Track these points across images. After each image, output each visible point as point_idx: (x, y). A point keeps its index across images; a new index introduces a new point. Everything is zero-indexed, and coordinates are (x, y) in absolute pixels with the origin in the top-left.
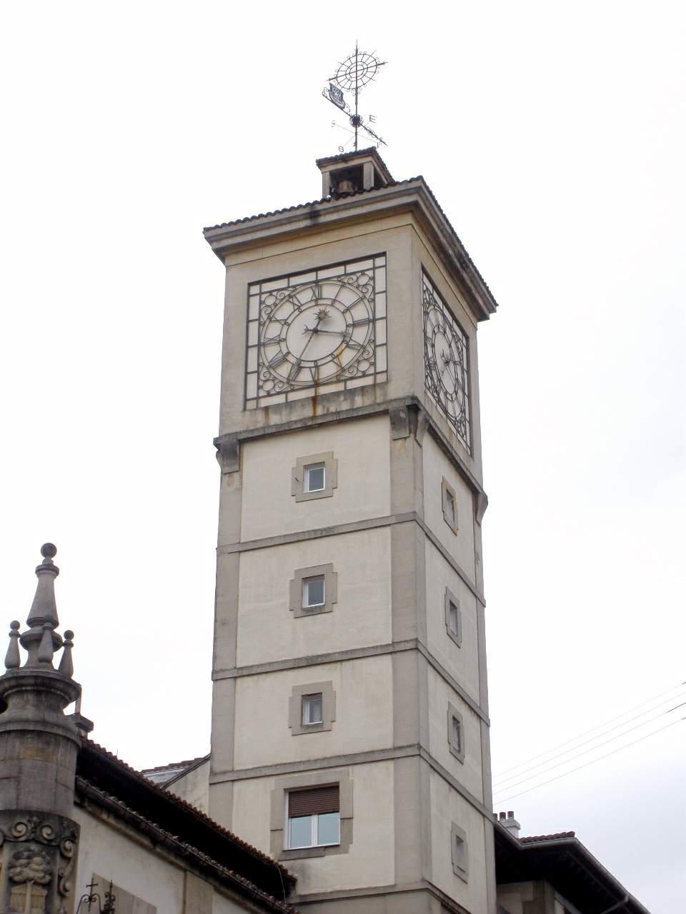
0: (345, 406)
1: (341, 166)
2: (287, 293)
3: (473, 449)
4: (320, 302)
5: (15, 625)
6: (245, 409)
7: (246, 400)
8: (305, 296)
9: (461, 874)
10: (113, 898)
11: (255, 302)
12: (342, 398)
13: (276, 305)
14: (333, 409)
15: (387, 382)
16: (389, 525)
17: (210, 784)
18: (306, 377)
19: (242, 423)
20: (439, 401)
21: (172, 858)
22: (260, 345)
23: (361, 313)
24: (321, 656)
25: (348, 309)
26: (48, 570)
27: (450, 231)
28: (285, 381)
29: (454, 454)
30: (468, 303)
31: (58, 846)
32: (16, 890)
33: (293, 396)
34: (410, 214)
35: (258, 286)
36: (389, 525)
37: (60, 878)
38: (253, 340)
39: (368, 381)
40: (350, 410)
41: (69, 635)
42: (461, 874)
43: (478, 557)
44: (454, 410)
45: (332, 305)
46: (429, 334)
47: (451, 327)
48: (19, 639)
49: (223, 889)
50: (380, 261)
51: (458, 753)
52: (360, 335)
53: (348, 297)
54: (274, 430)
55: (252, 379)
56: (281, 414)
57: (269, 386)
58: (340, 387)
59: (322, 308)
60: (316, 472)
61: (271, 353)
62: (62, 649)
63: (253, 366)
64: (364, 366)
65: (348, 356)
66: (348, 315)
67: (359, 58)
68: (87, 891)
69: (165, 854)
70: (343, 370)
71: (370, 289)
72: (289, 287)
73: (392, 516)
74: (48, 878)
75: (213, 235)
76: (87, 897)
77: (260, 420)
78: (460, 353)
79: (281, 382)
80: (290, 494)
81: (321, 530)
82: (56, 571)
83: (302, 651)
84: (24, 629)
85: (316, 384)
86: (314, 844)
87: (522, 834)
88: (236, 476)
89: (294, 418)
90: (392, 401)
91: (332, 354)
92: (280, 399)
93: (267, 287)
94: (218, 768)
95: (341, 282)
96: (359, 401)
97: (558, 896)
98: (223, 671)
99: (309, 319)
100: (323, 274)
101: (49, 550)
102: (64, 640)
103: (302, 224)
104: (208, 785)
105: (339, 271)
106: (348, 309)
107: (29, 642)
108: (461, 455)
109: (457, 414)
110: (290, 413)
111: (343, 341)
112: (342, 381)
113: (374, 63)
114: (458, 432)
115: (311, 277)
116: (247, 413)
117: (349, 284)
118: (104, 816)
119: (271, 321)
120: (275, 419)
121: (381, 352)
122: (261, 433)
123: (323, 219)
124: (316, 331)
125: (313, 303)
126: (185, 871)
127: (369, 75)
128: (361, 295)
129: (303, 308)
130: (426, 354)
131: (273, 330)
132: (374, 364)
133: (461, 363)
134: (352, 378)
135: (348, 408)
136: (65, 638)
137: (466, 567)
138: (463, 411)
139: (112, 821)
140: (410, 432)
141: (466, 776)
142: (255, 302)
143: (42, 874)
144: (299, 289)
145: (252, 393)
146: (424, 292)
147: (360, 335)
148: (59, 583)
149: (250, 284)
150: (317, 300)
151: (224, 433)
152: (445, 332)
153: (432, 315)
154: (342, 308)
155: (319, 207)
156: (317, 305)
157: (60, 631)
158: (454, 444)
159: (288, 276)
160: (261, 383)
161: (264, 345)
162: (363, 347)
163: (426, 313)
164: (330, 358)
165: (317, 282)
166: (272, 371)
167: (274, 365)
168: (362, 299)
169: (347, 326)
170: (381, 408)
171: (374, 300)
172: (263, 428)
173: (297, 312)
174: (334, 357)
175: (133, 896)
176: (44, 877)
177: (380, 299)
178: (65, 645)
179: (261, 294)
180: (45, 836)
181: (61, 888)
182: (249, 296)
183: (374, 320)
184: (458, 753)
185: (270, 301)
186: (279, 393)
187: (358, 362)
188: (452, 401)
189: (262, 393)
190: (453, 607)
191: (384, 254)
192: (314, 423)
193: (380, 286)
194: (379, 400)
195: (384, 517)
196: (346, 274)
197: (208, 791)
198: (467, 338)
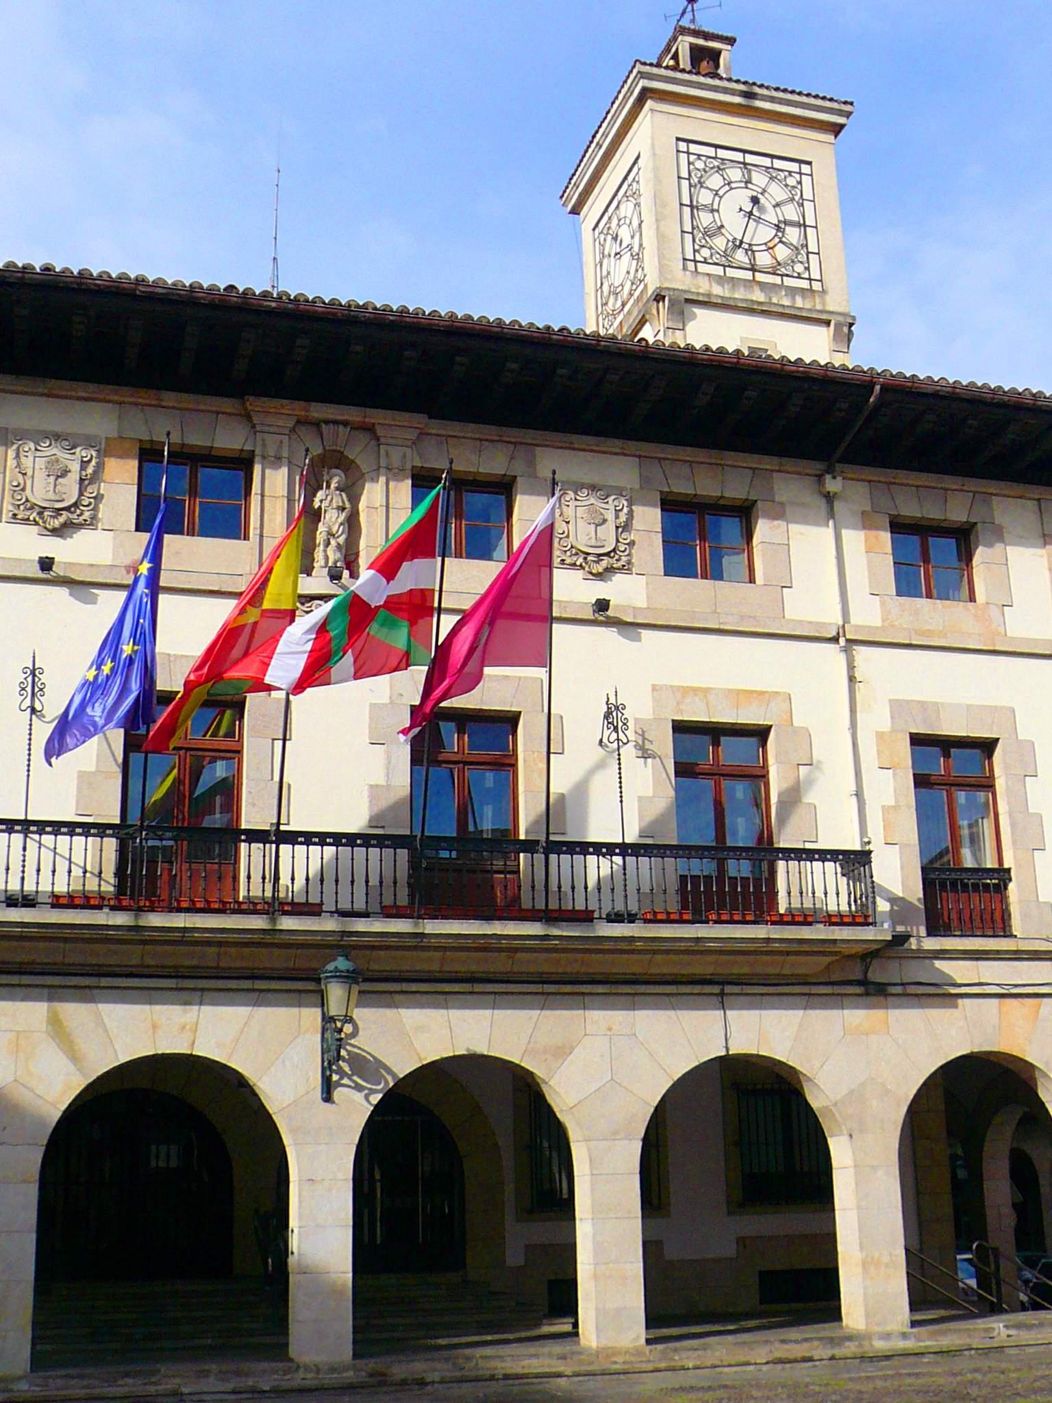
0: (786, 302)
1: (701, 42)
8: (735, 174)
14: (775, 300)
23: (791, 212)
25: (777, 205)
33: (731, 272)
38: (686, 201)
39: (804, 284)
50: (806, 169)
53: (777, 192)
54: (720, 301)
57: (705, 253)
63: (688, 228)
65: (782, 253)
66: (778, 209)
77: (703, 287)
90: (832, 313)
91: (765, 244)
92: (719, 271)
93: (694, 148)
96: (799, 302)
99: (742, 198)
100: (750, 159)
103: (738, 100)
111: (776, 235)
112: (778, 275)
119: (702, 186)
120: (717, 290)
125: (743, 185)
144: (729, 164)
147: (793, 234)
149: (678, 139)
150: (746, 183)
154: (774, 203)
155: (757, 90)
159: (717, 147)
160: (697, 247)
162: (797, 249)
164: (764, 247)
167: (708, 233)
168: (792, 200)
172: (709, 295)
182: (678, 151)
191: (810, 163)
193: (808, 194)
194: (819, 307)
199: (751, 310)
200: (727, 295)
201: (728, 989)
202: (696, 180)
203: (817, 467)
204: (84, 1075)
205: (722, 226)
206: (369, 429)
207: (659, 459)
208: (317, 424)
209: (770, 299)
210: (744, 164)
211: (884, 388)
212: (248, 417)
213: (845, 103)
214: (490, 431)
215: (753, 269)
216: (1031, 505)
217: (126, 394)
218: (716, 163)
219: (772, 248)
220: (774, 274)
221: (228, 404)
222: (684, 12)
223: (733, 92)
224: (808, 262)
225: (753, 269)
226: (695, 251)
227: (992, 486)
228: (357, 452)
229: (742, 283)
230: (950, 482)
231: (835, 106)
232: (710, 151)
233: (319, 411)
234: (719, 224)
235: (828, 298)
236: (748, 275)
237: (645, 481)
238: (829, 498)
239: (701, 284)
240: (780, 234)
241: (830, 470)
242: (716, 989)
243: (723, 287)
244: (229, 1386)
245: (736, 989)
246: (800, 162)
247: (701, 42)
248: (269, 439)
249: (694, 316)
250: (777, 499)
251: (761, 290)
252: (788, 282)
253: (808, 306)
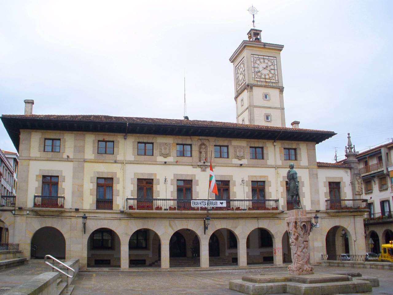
0: (272, 85)
1: (255, 32)
8: (262, 60)
14: (269, 85)
23: (272, 67)
26: (349, 138)
50: (275, 58)
57: (256, 76)
58: (270, 81)
64: (274, 78)
65: (271, 75)
77: (256, 83)
88: (252, 92)
93: (254, 56)
96: (274, 85)
100: (265, 57)
101: (349, 134)
103: (262, 46)
107: (348, 148)
120: (259, 83)
123: (266, 47)
124: (265, 68)
147: (272, 72)
168: (272, 65)
194: (277, 86)
199: (265, 87)
200: (261, 84)
201: (259, 219)
203: (273, 141)
204: (174, 231)
206: (208, 139)
207: (250, 141)
208: (201, 139)
210: (264, 58)
211: (283, 132)
212: (191, 139)
214: (225, 139)
215: (265, 79)
216: (306, 144)
217: (174, 137)
220: (269, 79)
221: (188, 137)
225: (265, 79)
227: (299, 142)
228: (206, 143)
230: (293, 142)
232: (257, 56)
233: (200, 137)
235: (279, 84)
236: (264, 80)
237: (247, 145)
238: (275, 146)
241: (275, 142)
242: (257, 219)
244: (194, 270)
245: (260, 219)
246: (274, 57)
248: (194, 142)
250: (267, 146)
253: (276, 85)
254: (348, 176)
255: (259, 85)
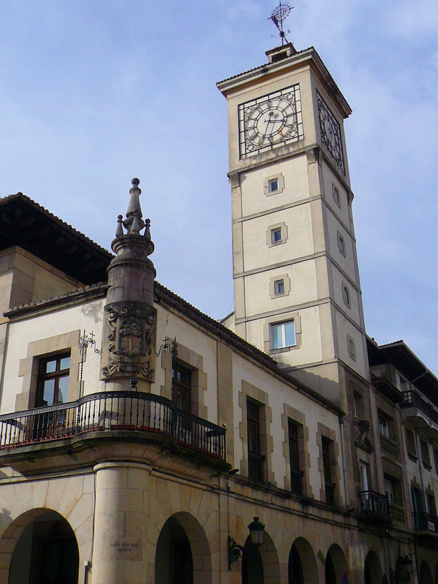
0: (285, 152)
1: (277, 53)
2: (255, 107)
3: (345, 172)
4: (271, 109)
5: (120, 217)
6: (240, 159)
7: (241, 155)
9: (352, 356)
10: (176, 345)
11: (242, 112)
12: (284, 149)
13: (251, 112)
14: (280, 154)
15: (304, 139)
16: (309, 202)
17: (235, 324)
18: (267, 142)
19: (239, 165)
20: (328, 149)
21: (210, 333)
22: (245, 131)
23: (290, 111)
24: (282, 263)
27: (328, 74)
28: (257, 145)
29: (337, 173)
30: (339, 110)
31: (145, 318)
32: (125, 339)
33: (261, 151)
34: (309, 65)
35: (243, 106)
36: (309, 202)
37: (147, 334)
38: (242, 129)
39: (296, 140)
40: (288, 153)
41: (148, 221)
42: (352, 356)
43: (351, 220)
44: (335, 154)
45: (276, 109)
46: (322, 119)
47: (331, 118)
48: (122, 224)
49: (237, 351)
50: (297, 87)
51: (348, 302)
52: (290, 121)
53: (284, 104)
54: (254, 166)
55: (243, 145)
56: (256, 159)
57: (250, 148)
59: (271, 111)
60: (273, 185)
61: (251, 133)
62: (145, 228)
63: (243, 140)
64: (293, 134)
65: (285, 130)
66: (284, 113)
67: (282, 7)
68: (164, 343)
69: (205, 331)
70: (283, 136)
71: (293, 99)
72: (256, 104)
73: (310, 198)
74: (140, 333)
75: (220, 85)
76: (164, 346)
77: (248, 163)
78: (336, 130)
79: (256, 145)
80: (263, 193)
81: (278, 208)
82: (140, 191)
83: (273, 262)
84: (124, 219)
85: (272, 144)
86: (284, 346)
87: (379, 345)
88: (238, 189)
89: (263, 160)
91: (278, 131)
93: (247, 105)
94: (238, 317)
95: (280, 98)
96: (291, 149)
97: (396, 370)
98: (237, 274)
100: (271, 97)
101: (136, 182)
102: (145, 224)
104: (234, 325)
105: (279, 94)
106: (284, 110)
107: (127, 225)
108: (340, 173)
109: (337, 157)
110: (261, 158)
111: (283, 124)
112: (283, 142)
113: (288, 8)
114: (338, 164)
115: (266, 98)
116: (241, 160)
117: (284, 99)
118: (172, 309)
120: (254, 162)
121: (300, 126)
122: (248, 168)
125: (268, 110)
126: (217, 340)
127: (287, 14)
128: (289, 103)
129: (263, 112)
130: (321, 127)
131: (251, 124)
132: (298, 132)
133: (337, 134)
134: (288, 140)
135: (287, 153)
136: (146, 222)
137: (346, 223)
138: (340, 156)
139: (176, 312)
140: (316, 160)
141: (352, 313)
142: (242, 112)
143: (137, 331)
144: (261, 104)
145: (243, 152)
146: (318, 100)
148: (141, 198)
149: (239, 105)
151: (232, 170)
152: (329, 120)
153: (322, 111)
154: (281, 110)
155: (268, 66)
156: (269, 110)
157: (144, 219)
158: (337, 169)
159: (256, 99)
161: (247, 130)
163: (320, 110)
164: (277, 132)
165: (269, 100)
166: (251, 141)
168: (290, 105)
169: (284, 117)
170: (302, 151)
171: (295, 105)
172: (249, 166)
173: (261, 114)
174: (279, 131)
175: (190, 350)
176: (138, 333)
177: (298, 104)
178: (146, 226)
179: (244, 109)
180: (138, 313)
181: (148, 339)
183: (296, 113)
184: (348, 302)
185: (249, 111)
186: (255, 150)
187: (290, 132)
188: (334, 150)
189: (248, 151)
190: (341, 240)
191: (298, 84)
192: (272, 161)
194: (301, 147)
195: (307, 199)
196: (282, 95)
197: (234, 328)
198: (339, 125)
199: (270, 163)
202: (247, 118)
205: (258, 132)
209: (278, 154)
213: (309, 49)
218: (255, 107)
219: (280, 131)
222: (283, 40)
223: (258, 73)
224: (298, 130)
226: (246, 149)
229: (265, 154)
231: (304, 53)
232: (254, 103)
234: (257, 132)
236: (270, 148)
239: (247, 163)
240: (284, 123)
243: (256, 159)
246: (294, 86)
247: (277, 53)
249: (246, 177)
251: (273, 153)
252: (287, 142)
253: (295, 149)
254: (97, 321)
255: (254, 164)
